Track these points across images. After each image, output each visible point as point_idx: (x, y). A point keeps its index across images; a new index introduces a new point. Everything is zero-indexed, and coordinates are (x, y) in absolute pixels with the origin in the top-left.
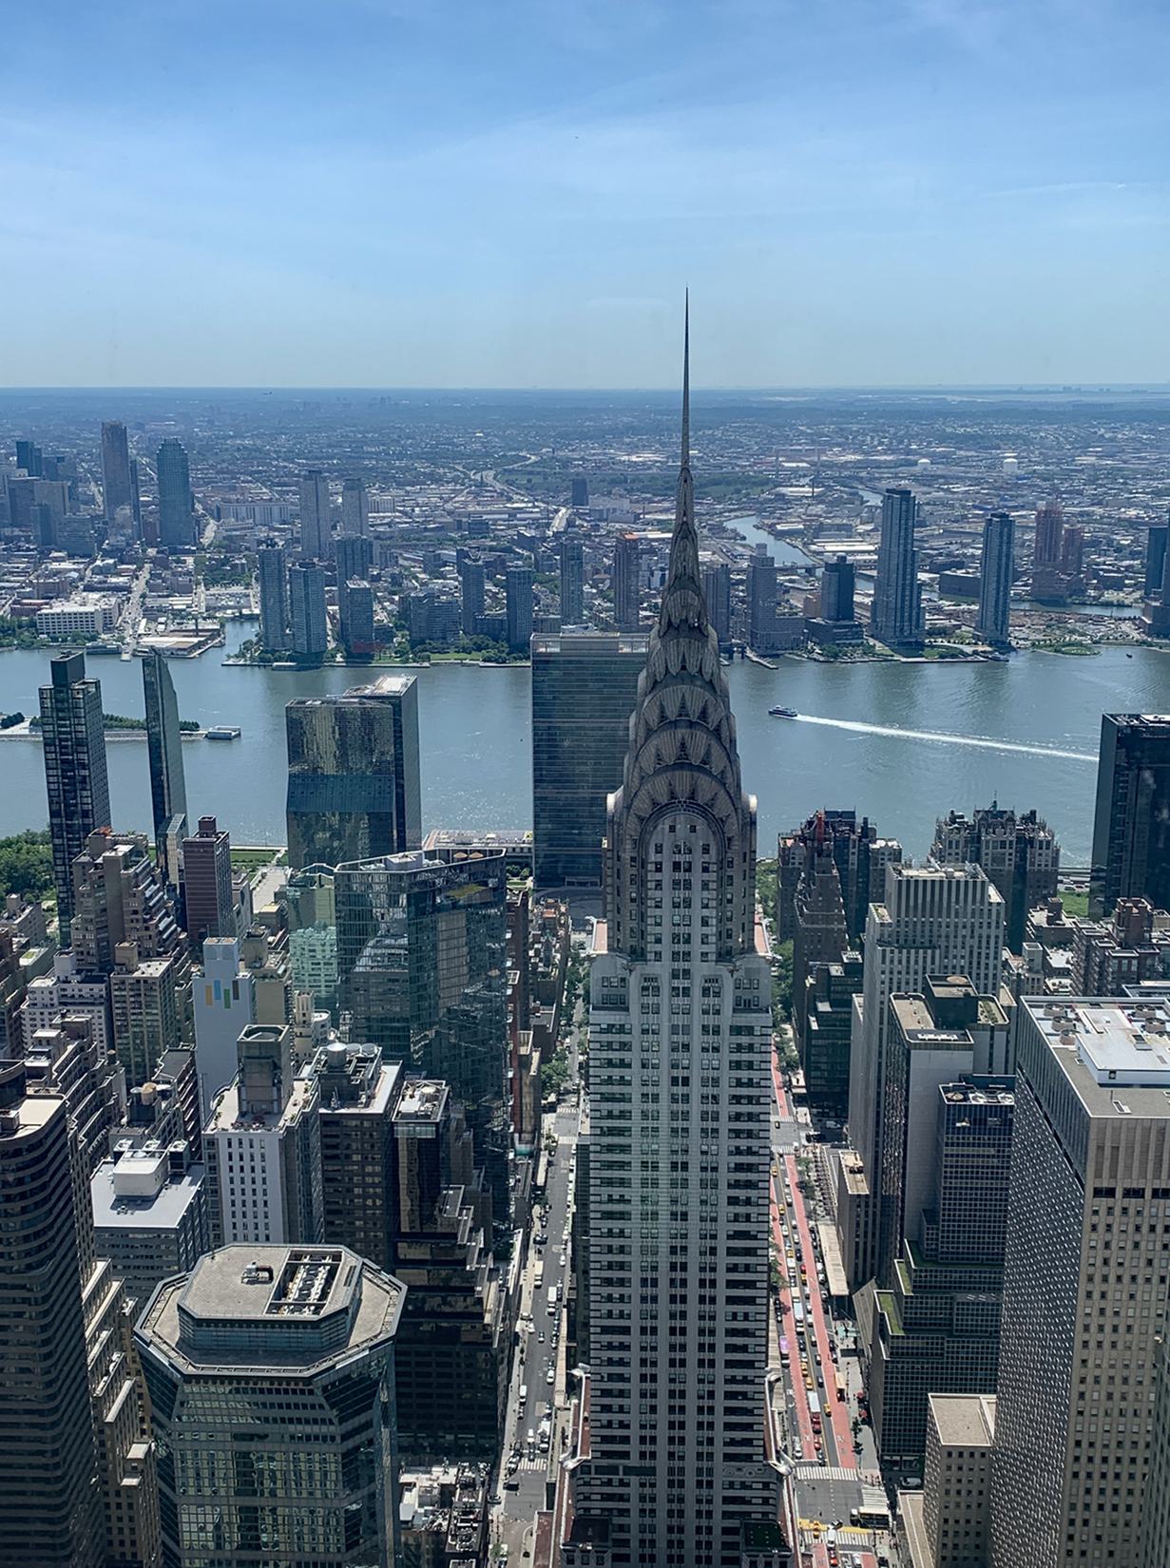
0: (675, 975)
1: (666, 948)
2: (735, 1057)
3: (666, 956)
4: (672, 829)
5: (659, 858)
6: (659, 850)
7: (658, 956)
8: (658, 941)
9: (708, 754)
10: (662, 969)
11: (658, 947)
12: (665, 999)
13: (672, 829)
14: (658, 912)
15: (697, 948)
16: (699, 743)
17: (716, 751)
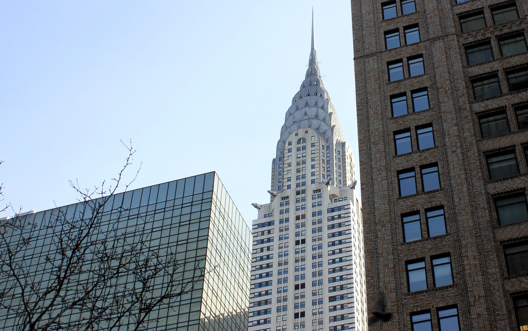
0: (298, 193)
1: (293, 183)
2: (331, 223)
3: (293, 186)
4: (297, 135)
5: (290, 147)
6: (290, 144)
7: (289, 187)
8: (289, 180)
9: (318, 111)
10: (291, 193)
11: (289, 183)
12: (292, 206)
13: (297, 135)
14: (289, 168)
15: (309, 178)
16: (312, 111)
17: (321, 111)
